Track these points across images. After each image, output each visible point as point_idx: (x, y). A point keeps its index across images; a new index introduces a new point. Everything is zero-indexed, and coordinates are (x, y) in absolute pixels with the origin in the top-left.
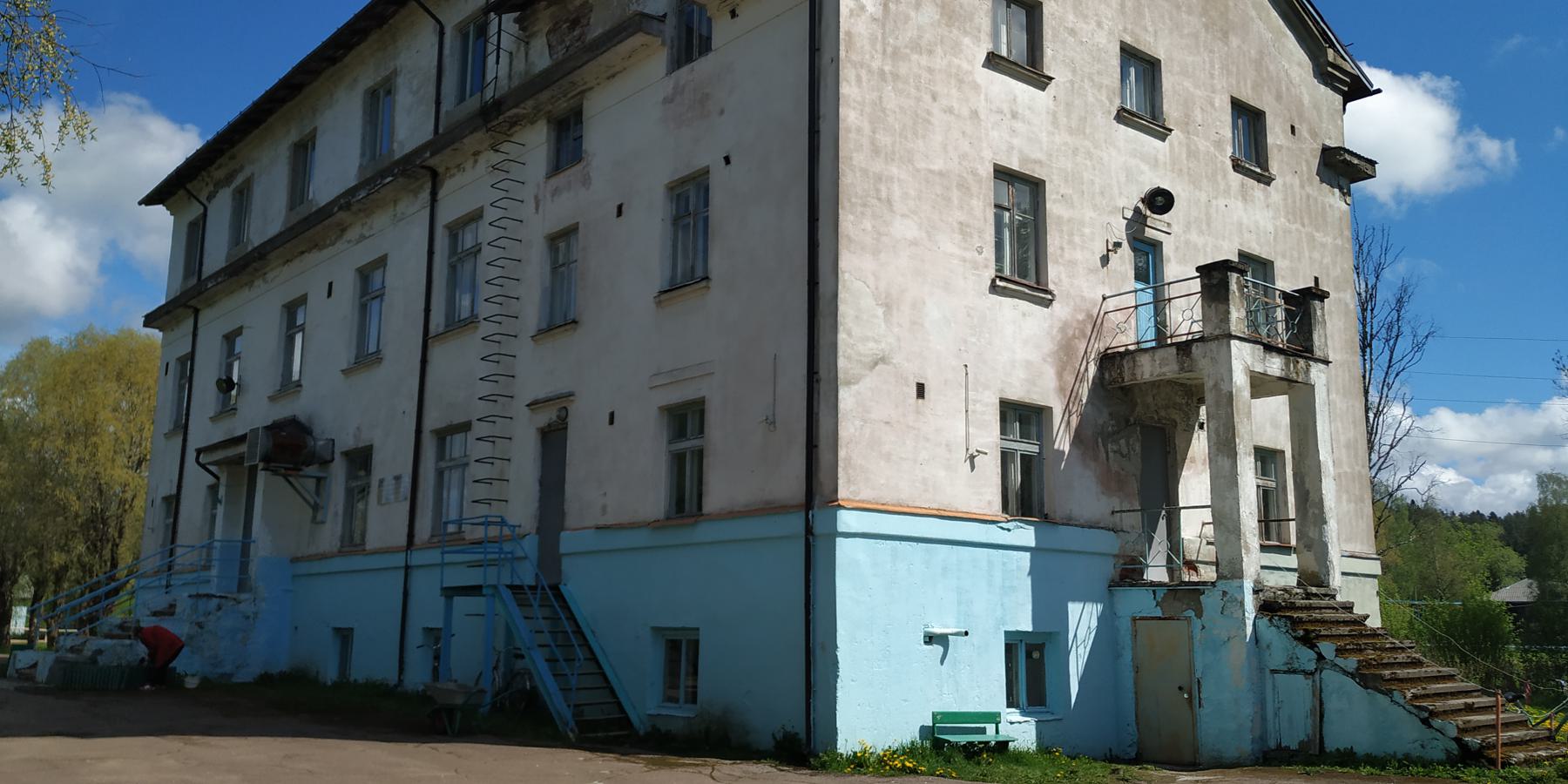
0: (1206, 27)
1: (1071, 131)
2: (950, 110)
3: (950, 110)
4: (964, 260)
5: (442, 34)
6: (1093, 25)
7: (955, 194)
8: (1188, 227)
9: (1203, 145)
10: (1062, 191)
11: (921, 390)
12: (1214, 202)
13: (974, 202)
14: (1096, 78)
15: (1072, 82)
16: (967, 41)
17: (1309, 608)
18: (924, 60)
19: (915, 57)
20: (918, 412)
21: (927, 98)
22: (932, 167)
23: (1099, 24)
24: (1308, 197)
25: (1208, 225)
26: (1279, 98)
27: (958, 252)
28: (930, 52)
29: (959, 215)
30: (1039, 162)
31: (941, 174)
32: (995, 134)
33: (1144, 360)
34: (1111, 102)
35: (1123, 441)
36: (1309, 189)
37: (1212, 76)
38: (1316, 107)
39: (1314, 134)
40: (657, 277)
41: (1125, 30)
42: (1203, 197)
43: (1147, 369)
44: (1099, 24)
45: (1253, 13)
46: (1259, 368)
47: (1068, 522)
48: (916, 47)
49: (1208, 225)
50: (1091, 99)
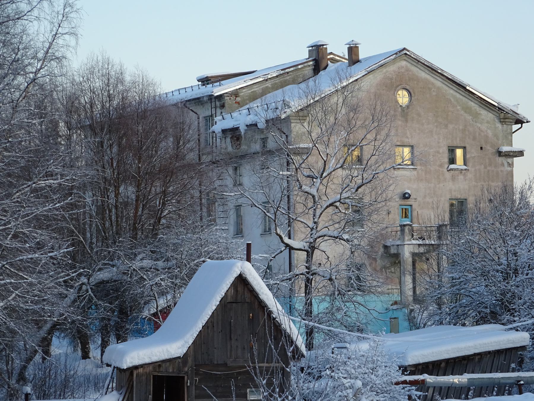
0: (437, 127)
5: (199, 118)
8: (425, 197)
12: (438, 186)
24: (488, 171)
26: (474, 139)
33: (392, 247)
35: (393, 269)
36: (489, 168)
37: (439, 143)
38: (496, 136)
40: (260, 231)
41: (397, 141)
42: (432, 185)
43: (393, 251)
45: (462, 112)
46: (416, 251)
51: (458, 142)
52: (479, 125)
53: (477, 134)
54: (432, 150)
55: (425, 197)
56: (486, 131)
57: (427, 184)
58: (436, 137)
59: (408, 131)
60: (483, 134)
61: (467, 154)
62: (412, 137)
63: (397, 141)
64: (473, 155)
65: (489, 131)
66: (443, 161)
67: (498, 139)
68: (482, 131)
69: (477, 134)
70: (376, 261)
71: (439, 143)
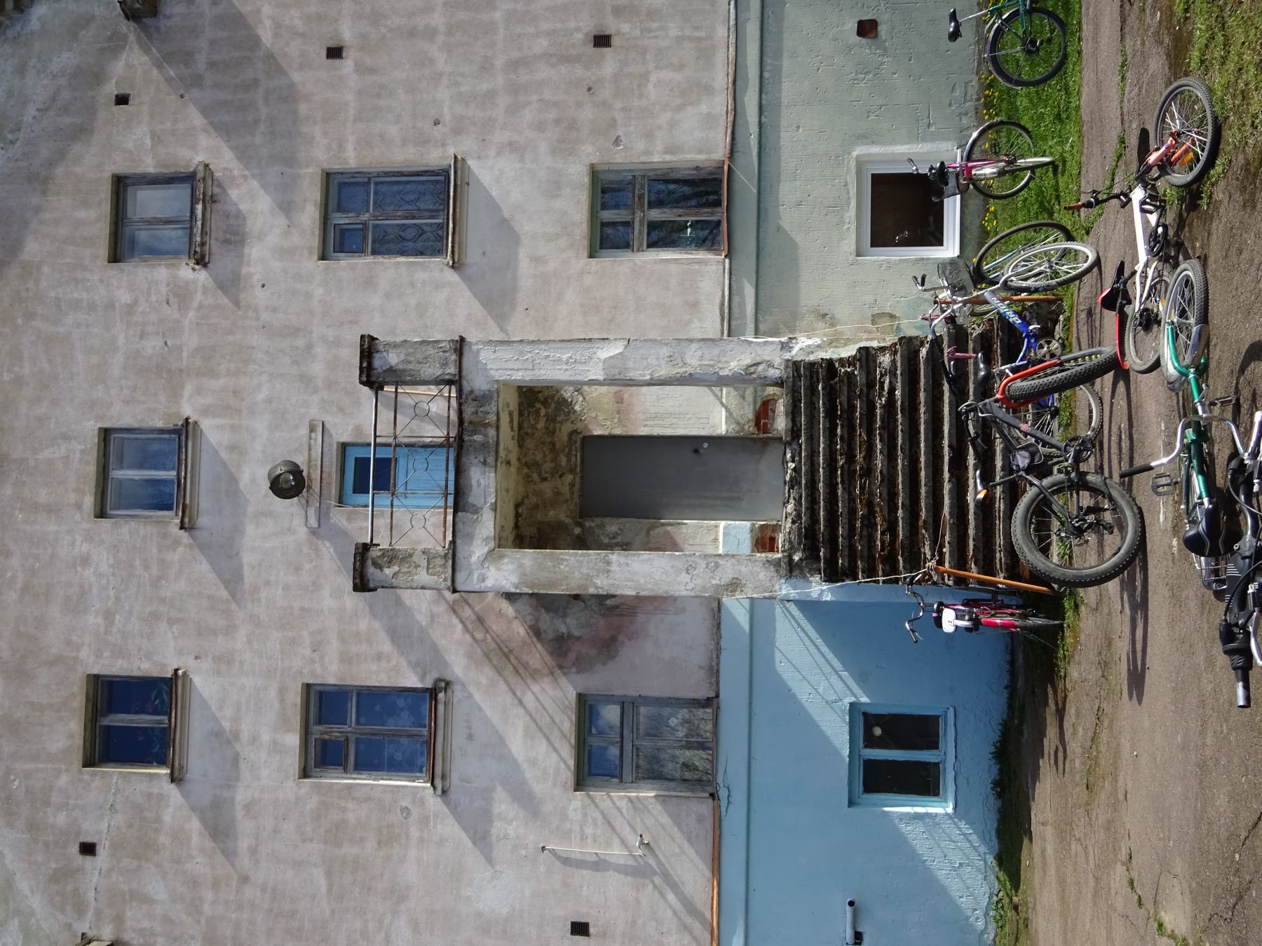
1: (230, 630)
2: (254, 851)
3: (254, 851)
4: (421, 840)
6: (88, 573)
7: (349, 850)
9: (191, 340)
10: (308, 652)
11: (580, 929)
12: (265, 316)
13: (351, 817)
14: (155, 571)
15: (171, 622)
16: (167, 817)
17: (812, 484)
18: (208, 895)
19: (207, 908)
20: (604, 935)
21: (249, 892)
22: (324, 889)
23: (85, 561)
25: (296, 331)
27: (412, 853)
28: (194, 883)
29: (371, 844)
30: (282, 691)
31: (329, 874)
32: (264, 773)
34: (177, 543)
36: (201, 61)
39: (114, 46)
41: (79, 506)
44: (85, 561)
47: (714, 672)
48: (194, 908)
49: (296, 331)
50: (181, 585)
51: (91, 214)
52: (31, 111)
53: (67, 120)
54: (121, 341)
55: (306, 379)
56: (55, 77)
57: (252, 367)
58: (70, 320)
59: (40, 457)
60: (66, 95)
61: (140, 170)
62: (66, 437)
63: (79, 506)
64: (148, 141)
65: (55, 65)
66: (164, 290)
67: (88, 20)
68: (53, 99)
69: (67, 120)
70: (570, 636)
71: (92, 307)
